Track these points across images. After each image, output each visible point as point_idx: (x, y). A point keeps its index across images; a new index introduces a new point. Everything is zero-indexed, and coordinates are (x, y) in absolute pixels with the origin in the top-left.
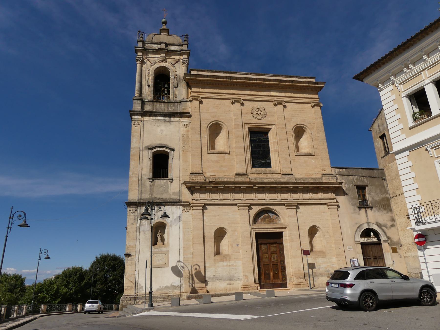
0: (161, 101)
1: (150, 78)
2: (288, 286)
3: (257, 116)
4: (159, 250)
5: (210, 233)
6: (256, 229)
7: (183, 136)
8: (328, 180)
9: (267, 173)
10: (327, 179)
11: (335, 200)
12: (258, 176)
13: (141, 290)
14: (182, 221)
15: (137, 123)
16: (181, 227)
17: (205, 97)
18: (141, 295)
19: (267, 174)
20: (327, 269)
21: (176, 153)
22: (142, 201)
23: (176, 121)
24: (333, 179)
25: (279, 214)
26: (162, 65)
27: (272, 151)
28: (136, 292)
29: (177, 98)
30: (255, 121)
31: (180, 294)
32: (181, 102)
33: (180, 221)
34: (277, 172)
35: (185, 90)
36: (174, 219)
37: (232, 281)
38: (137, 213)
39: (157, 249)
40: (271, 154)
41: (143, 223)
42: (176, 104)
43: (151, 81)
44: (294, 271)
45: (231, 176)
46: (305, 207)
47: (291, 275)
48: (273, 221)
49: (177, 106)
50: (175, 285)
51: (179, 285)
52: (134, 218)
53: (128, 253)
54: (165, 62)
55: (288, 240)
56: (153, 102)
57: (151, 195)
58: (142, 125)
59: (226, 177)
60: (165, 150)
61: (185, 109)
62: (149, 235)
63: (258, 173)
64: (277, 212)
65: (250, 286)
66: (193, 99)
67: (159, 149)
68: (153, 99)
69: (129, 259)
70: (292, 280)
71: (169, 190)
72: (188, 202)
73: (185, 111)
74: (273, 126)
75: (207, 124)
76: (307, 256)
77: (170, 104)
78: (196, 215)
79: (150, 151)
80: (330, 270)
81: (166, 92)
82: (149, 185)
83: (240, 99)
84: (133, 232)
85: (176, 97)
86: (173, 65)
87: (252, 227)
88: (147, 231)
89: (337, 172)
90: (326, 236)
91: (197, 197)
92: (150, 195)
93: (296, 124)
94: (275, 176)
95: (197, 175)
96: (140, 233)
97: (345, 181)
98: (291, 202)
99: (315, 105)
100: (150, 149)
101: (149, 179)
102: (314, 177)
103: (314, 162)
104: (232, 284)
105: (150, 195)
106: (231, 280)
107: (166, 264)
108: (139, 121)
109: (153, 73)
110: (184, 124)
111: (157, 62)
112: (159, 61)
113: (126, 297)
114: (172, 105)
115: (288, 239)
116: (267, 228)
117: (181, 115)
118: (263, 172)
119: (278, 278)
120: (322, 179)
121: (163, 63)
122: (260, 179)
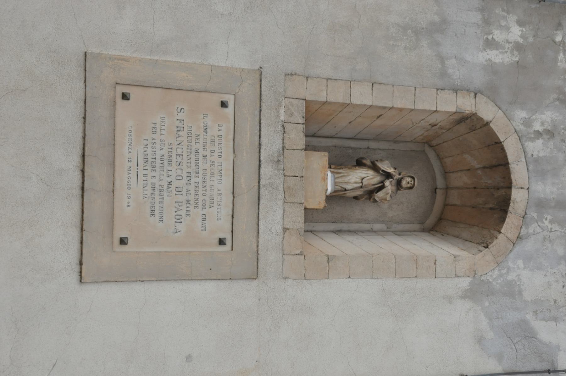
4: (267, 170)
39: (278, 145)
88: (442, 59)
107: (123, 241)
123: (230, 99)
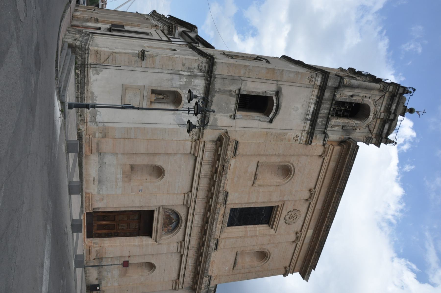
1: (360, 99)
2: (89, 239)
3: (289, 215)
5: (159, 162)
6: (159, 211)
7: (284, 134)
9: (222, 225)
10: (205, 282)
11: (181, 287)
12: (220, 215)
13: (95, 72)
14: (178, 128)
15: (312, 80)
16: (171, 126)
17: (324, 161)
18: (87, 72)
19: (221, 224)
21: (265, 125)
22: (212, 79)
23: (304, 127)
24: (204, 287)
25: (173, 235)
26: (371, 114)
27: (247, 228)
28: (92, 66)
29: (330, 128)
30: (284, 213)
31: (85, 121)
32: (325, 133)
33: (179, 125)
34: (222, 234)
35: (338, 138)
36: (183, 119)
37: (98, 182)
38: (196, 72)
40: (243, 227)
41: (184, 79)
42: (324, 127)
43: (357, 99)
44: (105, 249)
45: (226, 187)
46: (178, 260)
47: (101, 244)
48: (165, 227)
49: (321, 129)
50: (98, 116)
51: (97, 121)
52: (191, 68)
53: (146, 57)
54: (373, 117)
55: (142, 243)
56: (333, 100)
57: (219, 91)
58: (308, 86)
59: (226, 181)
60: (272, 112)
61: (316, 139)
62: (167, 86)
63: (224, 216)
64: (176, 232)
65: (90, 204)
66: (325, 149)
67: (275, 105)
68: (336, 99)
69: (137, 58)
70: (95, 246)
71: (222, 114)
72: (202, 138)
73: (314, 138)
74: (274, 231)
75: (293, 162)
76: (122, 264)
77: (325, 120)
78: (184, 146)
79: (274, 93)
80: (104, 281)
81: (339, 113)
82: (231, 89)
83: (313, 200)
84: (172, 66)
85: (331, 127)
86: (368, 126)
87: (161, 208)
88: (172, 83)
89: (211, 289)
91: (207, 148)
92: (218, 90)
93: (271, 252)
94: (218, 232)
95: (235, 150)
96: (171, 74)
98: (186, 247)
99: (287, 271)
100: (278, 93)
101: (239, 90)
102: (210, 269)
104: (94, 184)
105: (218, 90)
106: (99, 181)
108: (315, 83)
109: (365, 102)
110: (298, 137)
111: (376, 108)
112: (377, 111)
113: (87, 53)
114: (323, 122)
115: (143, 243)
116: (158, 223)
117: (311, 134)
118: (224, 220)
119: (98, 230)
120: (206, 277)
121: (373, 115)
122: (217, 218)
123: (140, 89)
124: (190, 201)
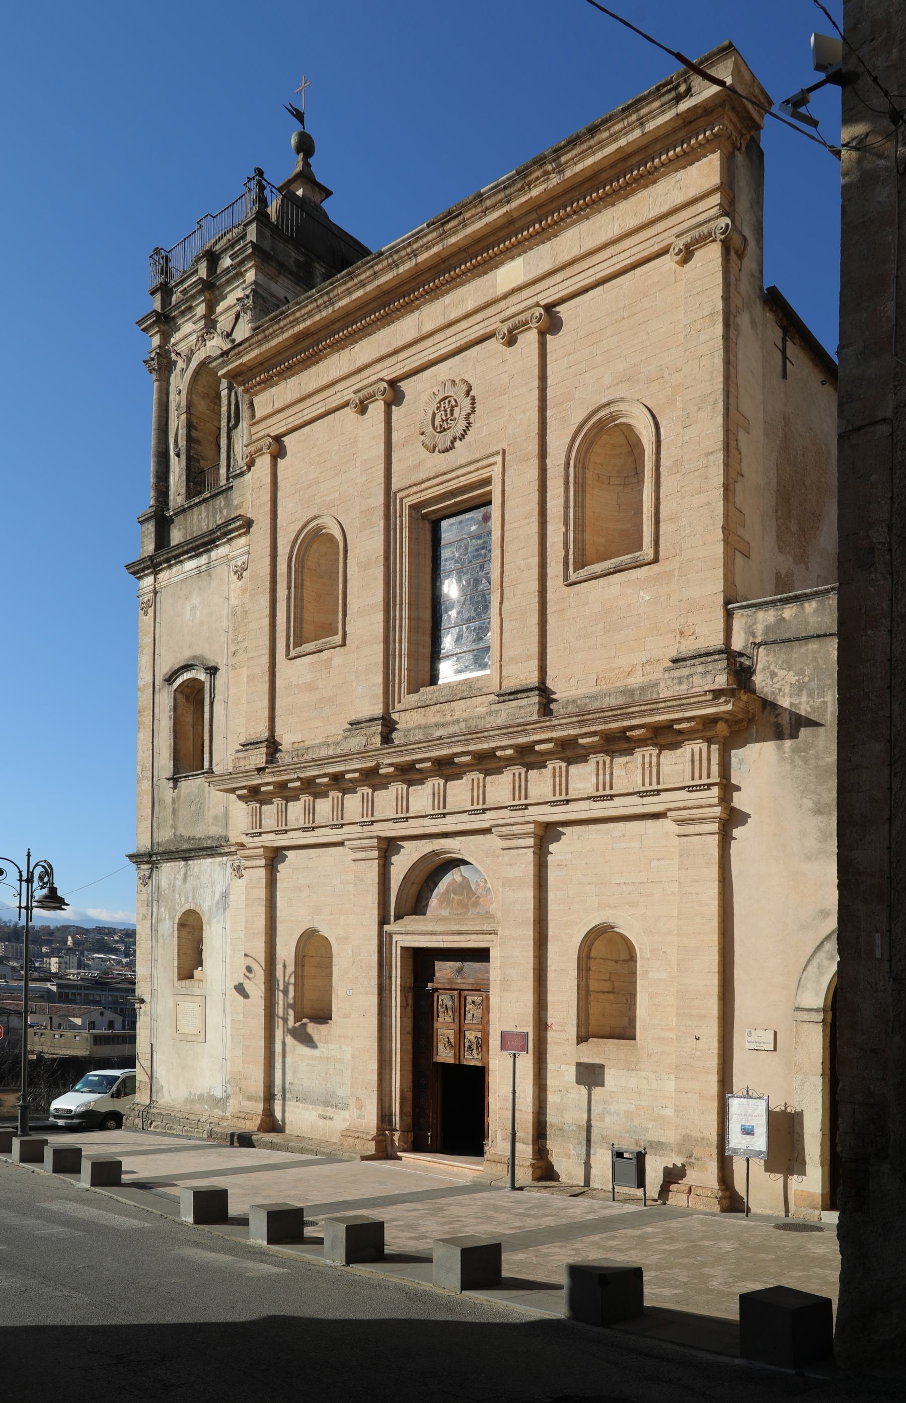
0: (198, 501)
8: (684, 687)
10: (680, 683)
20: (636, 1123)
80: (646, 1129)
90: (651, 975)
97: (800, 673)
103: (647, 598)
104: (331, 1119)
106: (327, 1104)
124: (362, 841)
